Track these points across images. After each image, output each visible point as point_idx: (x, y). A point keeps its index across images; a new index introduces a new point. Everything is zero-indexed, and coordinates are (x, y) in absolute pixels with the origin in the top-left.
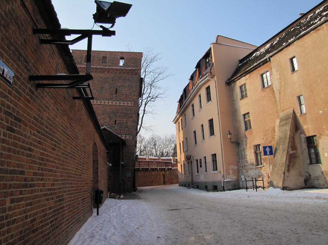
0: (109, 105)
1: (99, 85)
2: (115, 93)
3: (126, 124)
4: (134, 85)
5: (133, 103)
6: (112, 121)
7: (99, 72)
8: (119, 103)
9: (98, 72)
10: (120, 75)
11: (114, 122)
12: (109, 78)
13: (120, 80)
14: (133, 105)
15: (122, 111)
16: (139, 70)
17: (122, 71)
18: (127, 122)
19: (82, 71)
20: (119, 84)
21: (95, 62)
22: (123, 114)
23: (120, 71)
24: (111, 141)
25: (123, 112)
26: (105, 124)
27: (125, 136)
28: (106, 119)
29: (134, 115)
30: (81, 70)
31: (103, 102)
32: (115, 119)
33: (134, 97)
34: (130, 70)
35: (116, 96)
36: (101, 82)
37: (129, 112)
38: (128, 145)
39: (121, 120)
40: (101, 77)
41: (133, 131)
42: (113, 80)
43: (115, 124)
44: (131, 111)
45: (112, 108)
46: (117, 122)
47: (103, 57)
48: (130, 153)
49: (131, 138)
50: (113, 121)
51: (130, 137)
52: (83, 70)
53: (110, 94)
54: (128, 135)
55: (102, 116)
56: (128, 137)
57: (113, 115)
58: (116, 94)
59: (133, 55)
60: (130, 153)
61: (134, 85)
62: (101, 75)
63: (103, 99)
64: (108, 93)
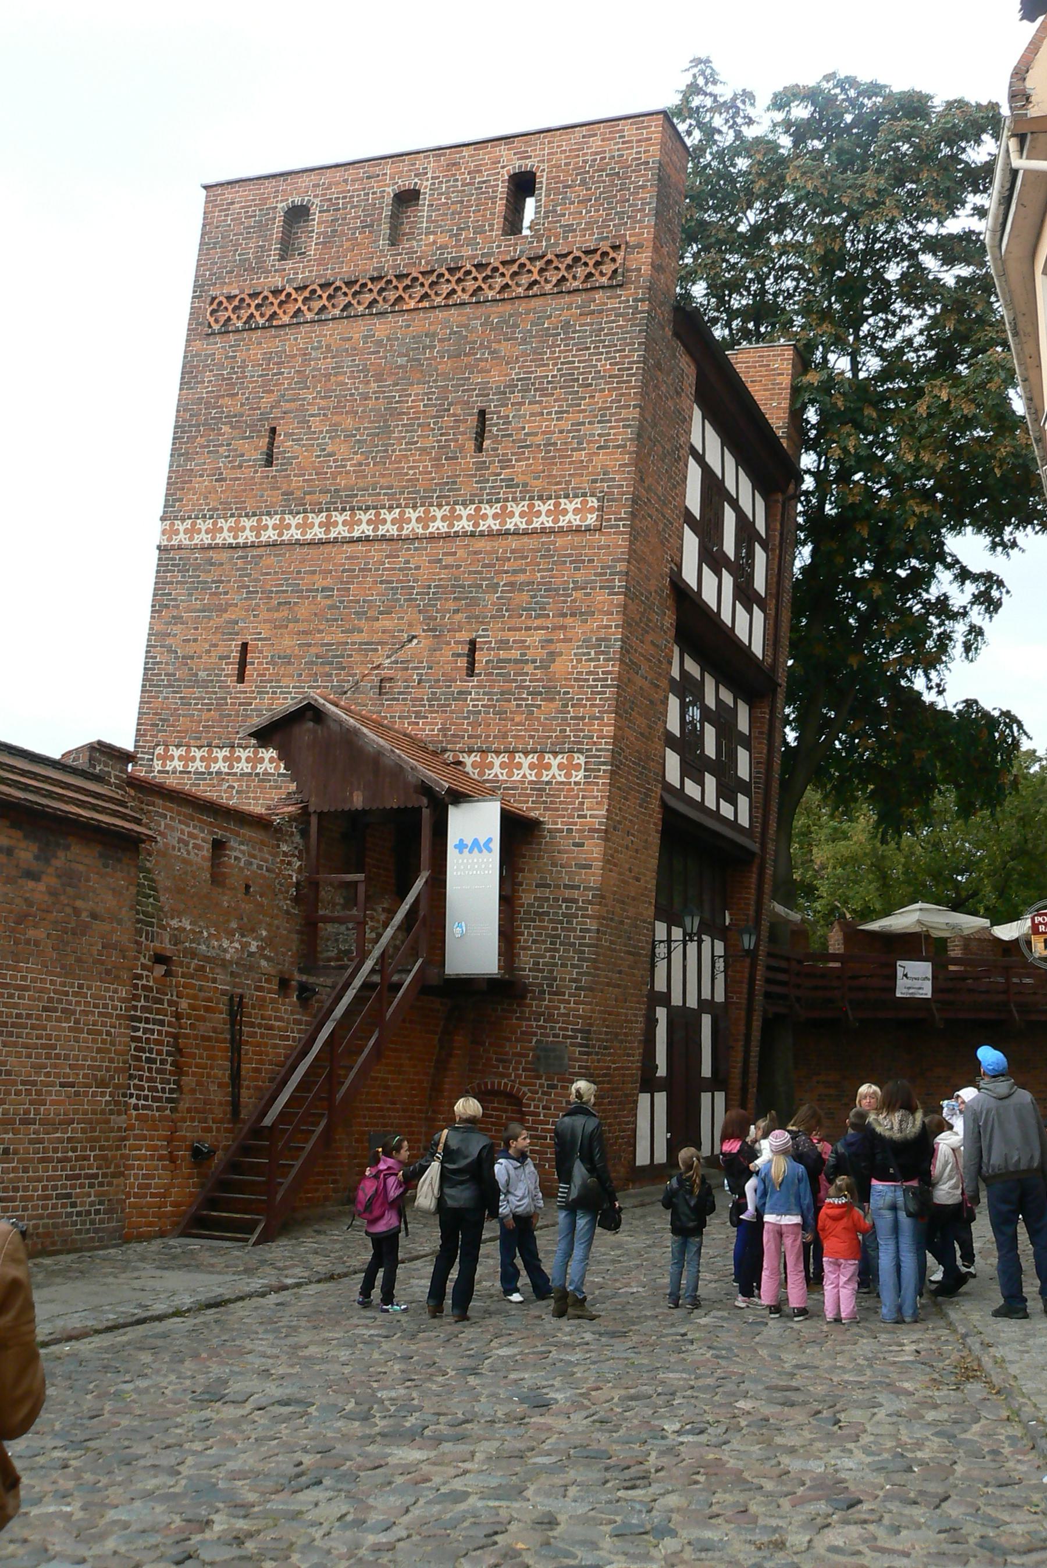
0: (432, 538)
1: (365, 397)
2: (471, 445)
3: (544, 666)
4: (603, 365)
5: (592, 502)
6: (447, 653)
7: (370, 305)
8: (495, 516)
9: (361, 308)
10: (507, 308)
11: (462, 663)
12: (434, 335)
13: (505, 348)
14: (591, 519)
15: (515, 572)
16: (640, 246)
17: (524, 280)
18: (553, 656)
19: (261, 321)
20: (496, 378)
21: (347, 245)
22: (525, 596)
23: (508, 274)
24: (358, 801)
25: (521, 578)
26: (399, 675)
27: (532, 758)
28: (410, 641)
29: (602, 597)
30: (257, 314)
31: (393, 522)
32: (465, 636)
33: (601, 459)
34: (577, 259)
35: (481, 466)
36: (379, 378)
37: (566, 575)
38: (550, 831)
39: (512, 636)
40: (379, 343)
41: (593, 718)
42: (456, 356)
43: (471, 671)
44: (577, 561)
45: (449, 560)
46: (481, 657)
47: (396, 195)
48: (567, 893)
49: (579, 776)
50: (459, 655)
51: (568, 768)
52: (268, 313)
53: (440, 459)
54: (555, 753)
55: (385, 623)
56: (555, 769)
57: (451, 605)
58: (479, 449)
59: (596, 143)
60: (566, 886)
61: (603, 365)
62: (381, 328)
63: (391, 496)
64: (423, 450)
